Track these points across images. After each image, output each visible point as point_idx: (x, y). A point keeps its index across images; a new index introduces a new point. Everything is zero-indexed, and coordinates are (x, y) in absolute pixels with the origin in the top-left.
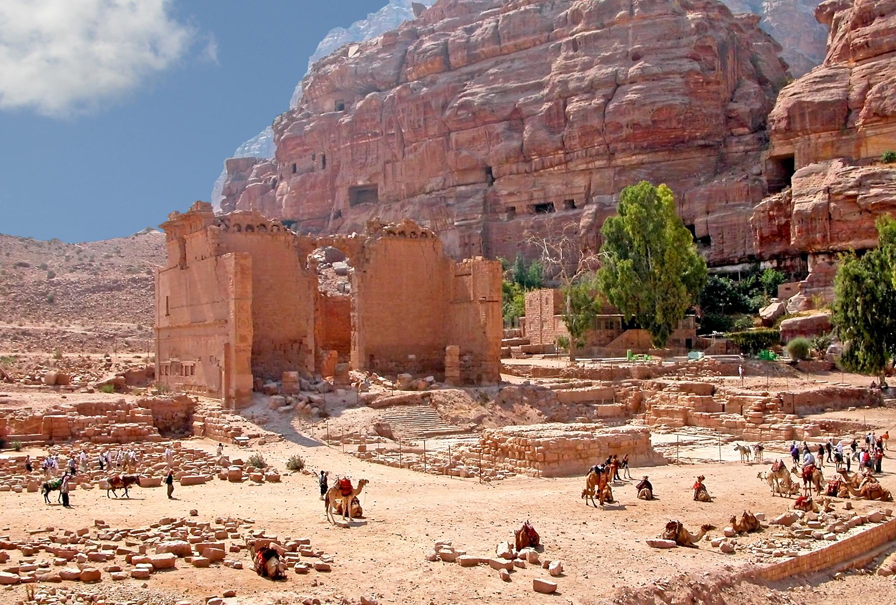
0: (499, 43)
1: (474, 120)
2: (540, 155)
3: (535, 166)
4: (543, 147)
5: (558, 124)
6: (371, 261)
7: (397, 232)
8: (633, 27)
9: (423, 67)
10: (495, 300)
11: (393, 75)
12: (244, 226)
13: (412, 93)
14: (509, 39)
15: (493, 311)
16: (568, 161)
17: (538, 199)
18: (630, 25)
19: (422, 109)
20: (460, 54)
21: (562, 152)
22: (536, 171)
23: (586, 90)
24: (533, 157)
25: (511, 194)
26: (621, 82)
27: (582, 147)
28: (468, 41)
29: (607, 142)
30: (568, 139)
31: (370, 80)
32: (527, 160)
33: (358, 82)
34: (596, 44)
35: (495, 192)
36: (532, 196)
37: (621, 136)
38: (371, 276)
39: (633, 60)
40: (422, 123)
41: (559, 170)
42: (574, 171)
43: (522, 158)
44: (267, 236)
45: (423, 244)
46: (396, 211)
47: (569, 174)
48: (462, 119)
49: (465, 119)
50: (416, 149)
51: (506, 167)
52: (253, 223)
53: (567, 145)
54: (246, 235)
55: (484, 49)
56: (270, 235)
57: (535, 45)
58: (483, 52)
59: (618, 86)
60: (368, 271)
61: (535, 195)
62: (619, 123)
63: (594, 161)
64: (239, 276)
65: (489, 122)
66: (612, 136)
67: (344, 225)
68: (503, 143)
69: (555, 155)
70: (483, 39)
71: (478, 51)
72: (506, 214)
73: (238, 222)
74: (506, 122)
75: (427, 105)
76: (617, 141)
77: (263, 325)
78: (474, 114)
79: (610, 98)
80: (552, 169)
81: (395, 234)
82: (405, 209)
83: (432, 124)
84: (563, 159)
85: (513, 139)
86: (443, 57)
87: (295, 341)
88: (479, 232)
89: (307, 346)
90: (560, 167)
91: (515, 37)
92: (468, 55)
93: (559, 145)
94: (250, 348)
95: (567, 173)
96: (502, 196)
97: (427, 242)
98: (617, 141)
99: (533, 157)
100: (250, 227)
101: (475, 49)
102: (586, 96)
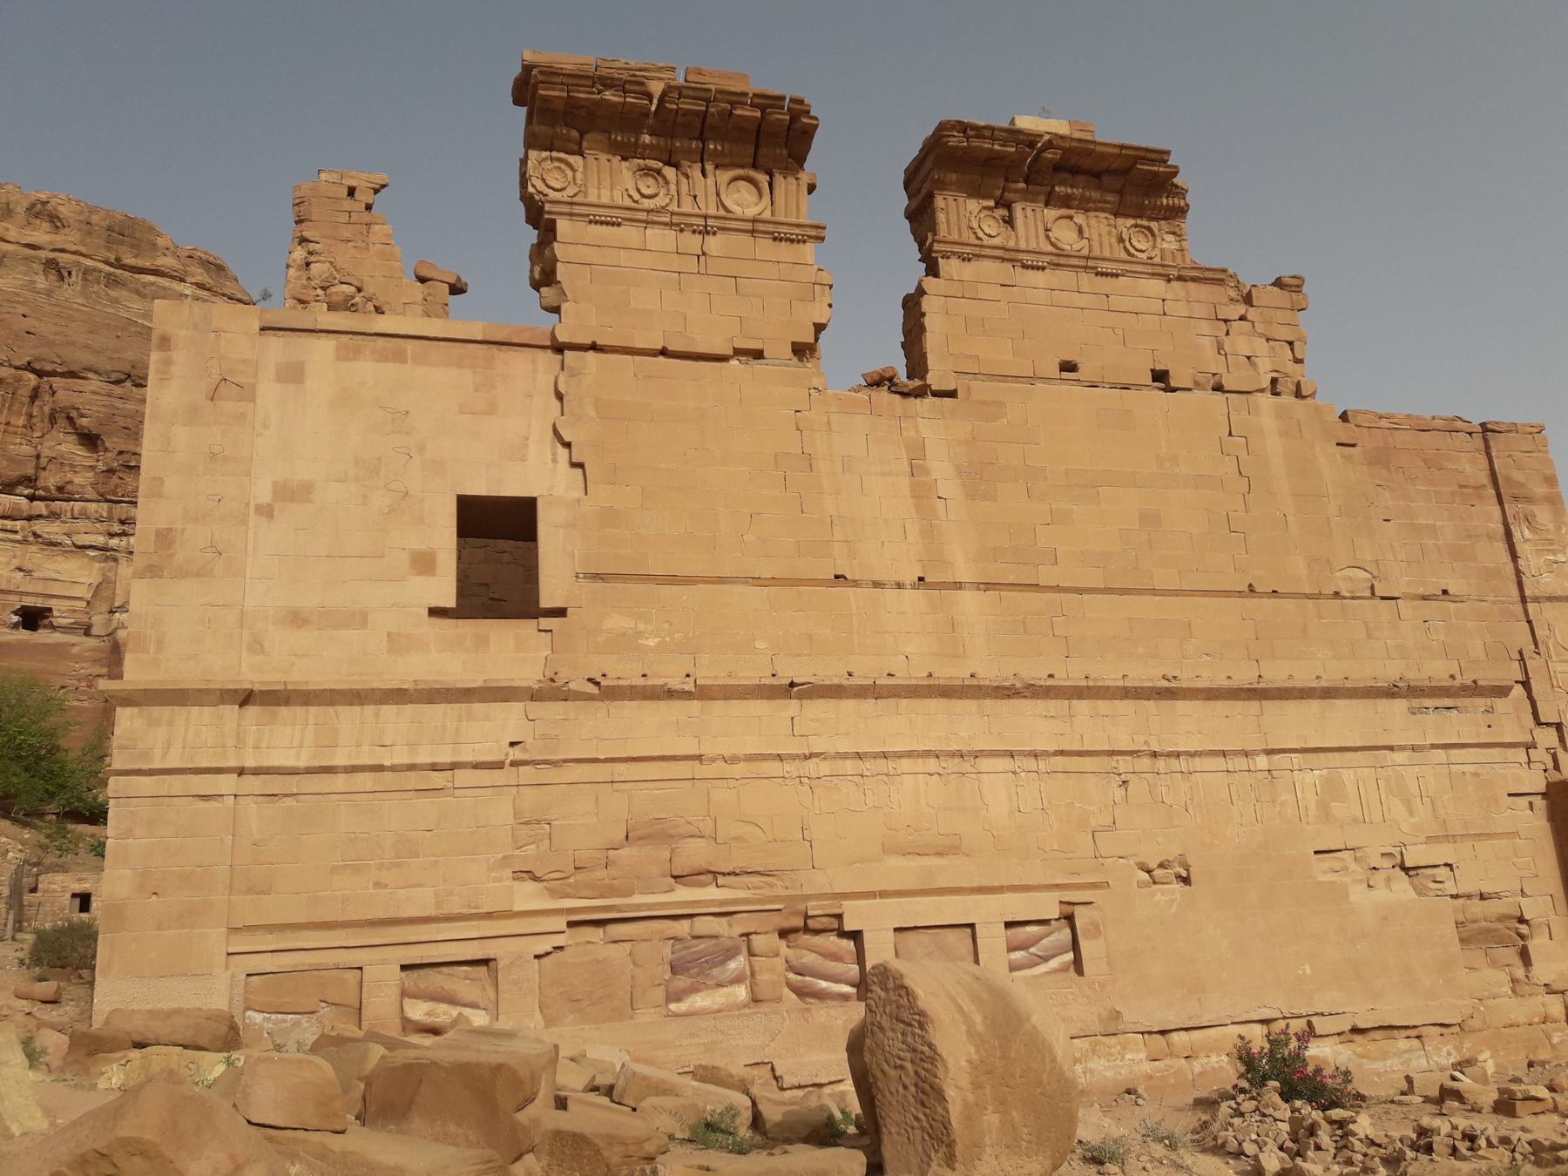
23: (114, 377)
95: (24, 541)
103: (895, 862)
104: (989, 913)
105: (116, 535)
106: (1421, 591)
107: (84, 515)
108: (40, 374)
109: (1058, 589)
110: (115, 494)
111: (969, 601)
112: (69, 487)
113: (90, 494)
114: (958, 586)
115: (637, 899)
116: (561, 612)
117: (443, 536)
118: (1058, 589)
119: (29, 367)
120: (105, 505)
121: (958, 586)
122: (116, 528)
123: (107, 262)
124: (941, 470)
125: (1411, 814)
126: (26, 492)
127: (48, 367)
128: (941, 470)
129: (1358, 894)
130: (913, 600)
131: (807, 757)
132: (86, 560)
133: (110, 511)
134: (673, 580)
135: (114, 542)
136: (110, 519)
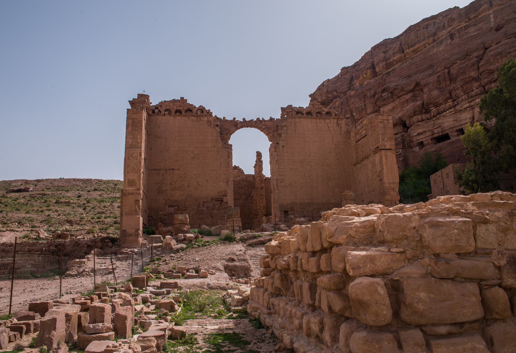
0: (403, 52)
1: (392, 97)
2: (436, 106)
3: (434, 113)
4: (437, 100)
5: (446, 85)
6: (283, 135)
7: (305, 112)
8: (494, 12)
9: (361, 78)
10: (387, 148)
11: (347, 87)
12: (173, 111)
13: (356, 91)
14: (409, 48)
15: (386, 159)
16: (456, 105)
17: (437, 133)
18: (491, 12)
19: (362, 99)
20: (381, 64)
21: (451, 100)
22: (434, 116)
24: (431, 109)
25: (419, 134)
26: (489, 46)
27: (464, 93)
28: (384, 57)
29: (483, 84)
30: (453, 91)
31: (335, 93)
32: (428, 111)
33: (330, 96)
34: (466, 31)
35: (409, 135)
36: (433, 132)
37: (493, 78)
38: (283, 146)
39: (496, 31)
40: (363, 107)
41: (450, 112)
42: (461, 110)
43: (424, 111)
44: (192, 118)
45: (328, 121)
47: (458, 114)
48: (385, 98)
49: (387, 97)
50: (361, 122)
51: (415, 119)
52: (182, 108)
53: (453, 94)
54: (175, 116)
55: (394, 58)
56: (195, 116)
57: (425, 47)
58: (394, 60)
59: (486, 49)
60: (281, 143)
61: (436, 131)
62: (491, 70)
63: (474, 100)
64: (130, 129)
65: (401, 96)
66: (486, 80)
68: (411, 104)
69: (446, 103)
70: (393, 53)
71: (391, 60)
72: (418, 147)
73: (168, 107)
74: (412, 93)
75: (365, 96)
76: (490, 82)
77: (189, 186)
78: (391, 93)
79: (481, 57)
80: (445, 113)
81: (302, 114)
83: (369, 107)
84: (452, 104)
85: (417, 101)
86: (371, 70)
87: (217, 200)
88: (402, 159)
89: (227, 203)
90: (450, 110)
91: (412, 46)
92: (386, 64)
93: (448, 95)
95: (455, 113)
96: (414, 136)
97: (332, 120)
98: (490, 82)
99: (431, 109)
100: (178, 112)
101: (389, 60)
102: (463, 61)
105: (471, 101)
107: (462, 100)
108: (449, 68)
110: (466, 91)
112: (457, 95)
113: (462, 94)
119: (445, 68)
120: (466, 95)
122: (470, 100)
123: (466, 22)
126: (451, 100)
127: (449, 66)
132: (468, 111)
133: (468, 96)
135: (472, 103)
136: (468, 98)
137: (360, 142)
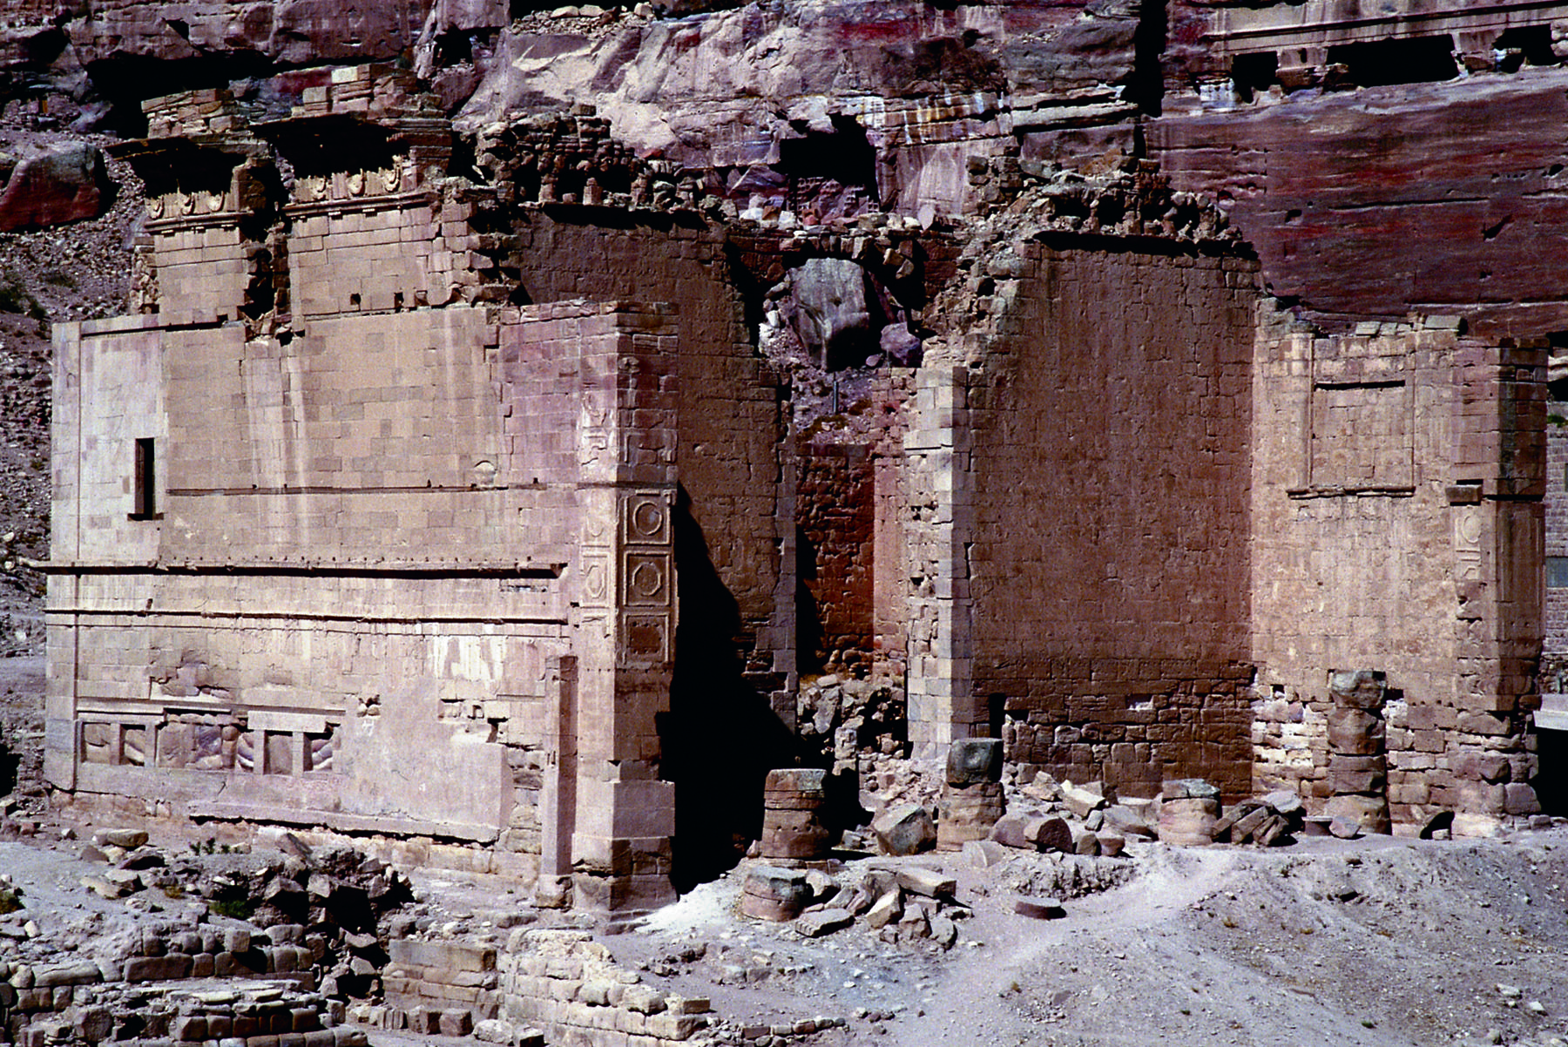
46: (726, 48)
67: (473, 99)
82: (762, 44)
94: (667, 678)
103: (269, 687)
104: (302, 723)
106: (520, 481)
109: (342, 491)
111: (303, 499)
114: (298, 491)
115: (187, 699)
116: (160, 516)
117: (129, 469)
118: (342, 491)
121: (298, 491)
124: (296, 396)
125: (492, 675)
128: (296, 396)
129: (460, 738)
130: (279, 502)
131: (237, 616)
134: (199, 492)
137: (1341, 397)
